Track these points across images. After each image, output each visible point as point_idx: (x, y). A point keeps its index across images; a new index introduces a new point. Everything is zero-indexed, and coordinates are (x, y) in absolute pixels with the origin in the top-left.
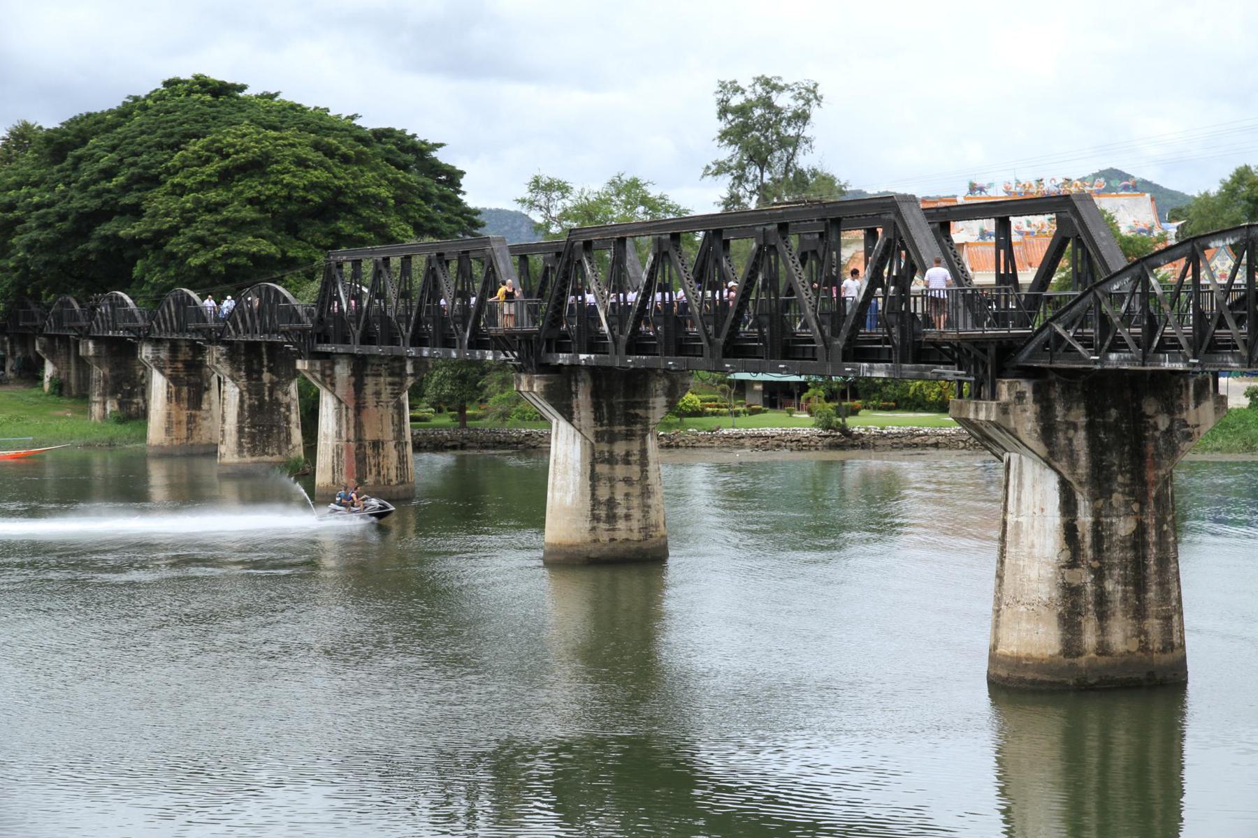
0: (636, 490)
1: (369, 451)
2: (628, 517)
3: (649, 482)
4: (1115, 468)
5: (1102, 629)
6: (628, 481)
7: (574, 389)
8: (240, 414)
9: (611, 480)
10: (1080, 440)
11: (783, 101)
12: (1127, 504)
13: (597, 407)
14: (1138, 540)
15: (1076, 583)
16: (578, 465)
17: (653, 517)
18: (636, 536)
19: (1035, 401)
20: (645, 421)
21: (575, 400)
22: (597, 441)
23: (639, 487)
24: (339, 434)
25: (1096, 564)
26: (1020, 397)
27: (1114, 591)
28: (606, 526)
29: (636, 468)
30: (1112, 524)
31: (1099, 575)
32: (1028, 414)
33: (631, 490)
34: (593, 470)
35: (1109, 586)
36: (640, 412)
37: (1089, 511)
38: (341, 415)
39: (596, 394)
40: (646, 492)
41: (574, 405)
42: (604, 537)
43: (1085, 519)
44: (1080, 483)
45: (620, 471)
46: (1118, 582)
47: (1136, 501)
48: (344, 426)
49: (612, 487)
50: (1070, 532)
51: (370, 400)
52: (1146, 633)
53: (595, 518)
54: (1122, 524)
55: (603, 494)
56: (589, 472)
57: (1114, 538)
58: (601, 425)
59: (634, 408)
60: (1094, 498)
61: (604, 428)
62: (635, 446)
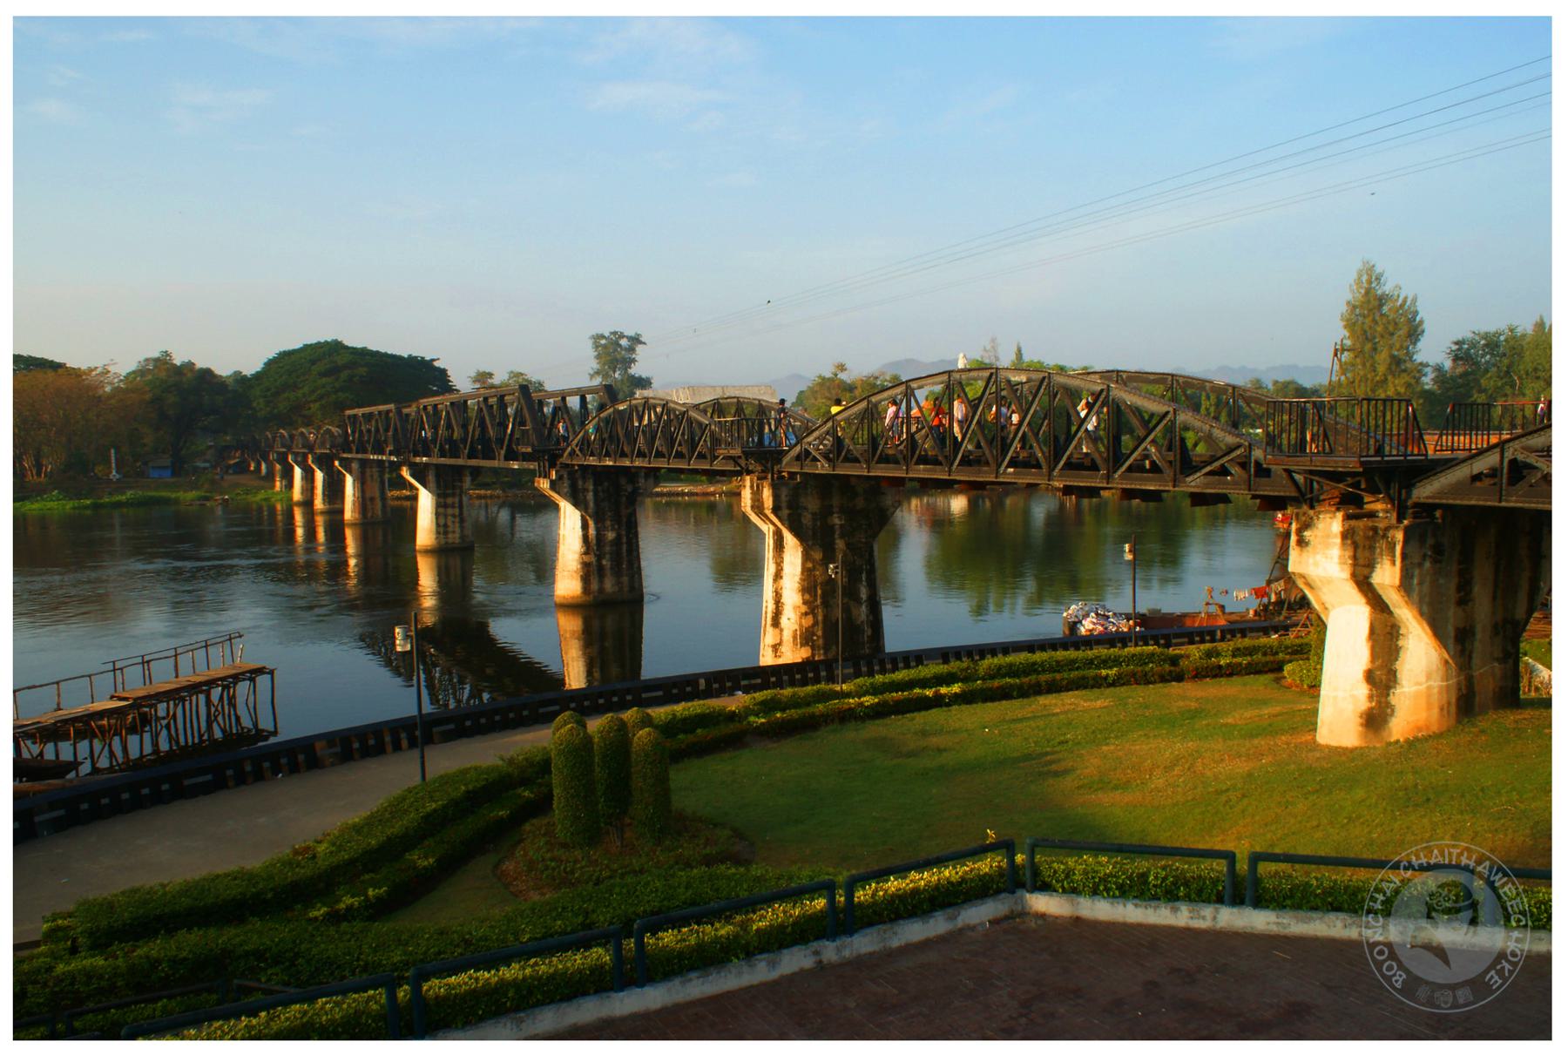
0: (457, 520)
1: (368, 503)
2: (454, 532)
5: (601, 582)
6: (454, 516)
8: (324, 486)
9: (446, 516)
10: (590, 496)
11: (624, 342)
12: (612, 525)
13: (438, 483)
14: (617, 542)
24: (354, 495)
26: (560, 478)
29: (457, 511)
31: (599, 558)
35: (604, 562)
40: (462, 521)
42: (443, 542)
43: (592, 531)
45: (450, 511)
49: (446, 518)
50: (585, 538)
51: (369, 479)
55: (442, 521)
60: (596, 523)
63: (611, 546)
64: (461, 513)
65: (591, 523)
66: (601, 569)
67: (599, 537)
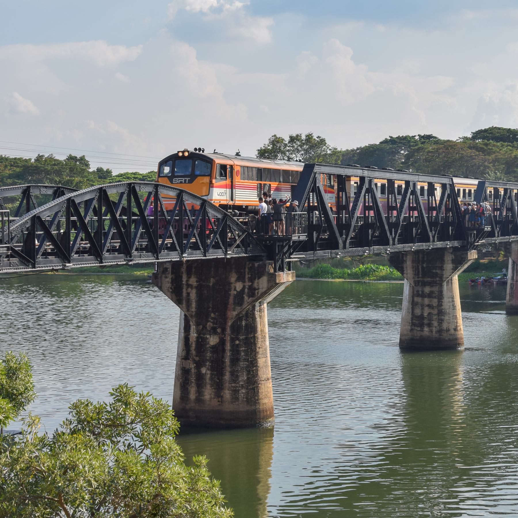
0: (435, 312)
2: (430, 325)
3: (443, 307)
4: (210, 309)
6: (429, 306)
7: (405, 259)
15: (187, 367)
16: (407, 297)
17: (445, 326)
18: (435, 335)
19: (173, 273)
20: (441, 277)
21: (405, 266)
22: (415, 285)
23: (436, 310)
25: (197, 359)
27: (206, 373)
28: (419, 329)
30: (207, 338)
31: (199, 365)
32: (168, 279)
33: (432, 311)
34: (413, 301)
35: (204, 370)
36: (439, 271)
37: (195, 331)
38: (514, 269)
41: (405, 267)
42: (419, 334)
43: (193, 335)
44: (192, 316)
45: (426, 301)
46: (208, 369)
47: (219, 327)
48: (515, 274)
50: (186, 341)
52: (222, 397)
53: (413, 324)
54: (212, 339)
55: (418, 312)
56: (411, 300)
57: (208, 346)
58: (418, 278)
59: (436, 269)
60: (197, 324)
61: (420, 279)
62: (436, 289)
63: (212, 352)
64: (440, 304)
65: (193, 327)
67: (201, 342)
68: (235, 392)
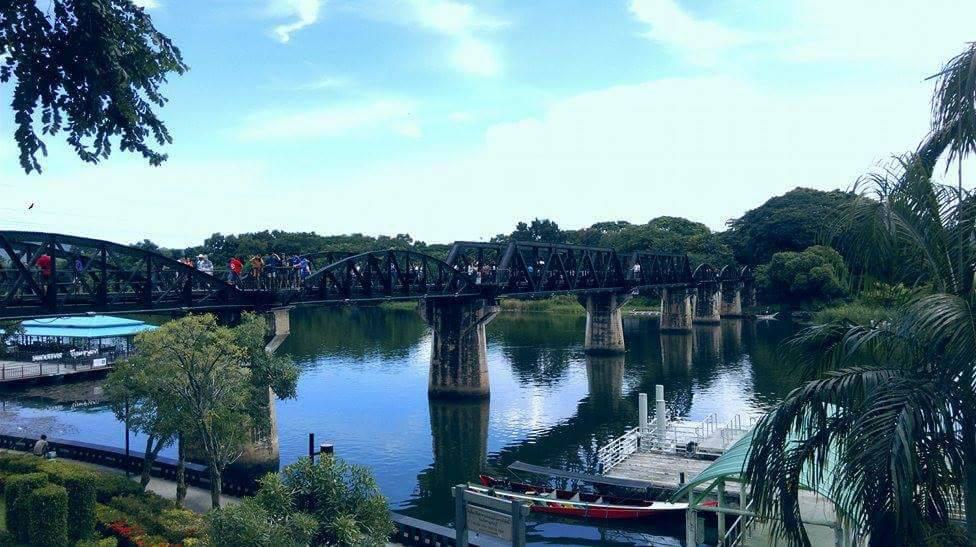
2: (602, 340)
10: (439, 320)
17: (612, 341)
18: (606, 347)
31: (443, 364)
39: (593, 300)
43: (440, 345)
55: (595, 332)
65: (439, 340)
66: (444, 371)
67: (444, 349)
68: (465, 380)
